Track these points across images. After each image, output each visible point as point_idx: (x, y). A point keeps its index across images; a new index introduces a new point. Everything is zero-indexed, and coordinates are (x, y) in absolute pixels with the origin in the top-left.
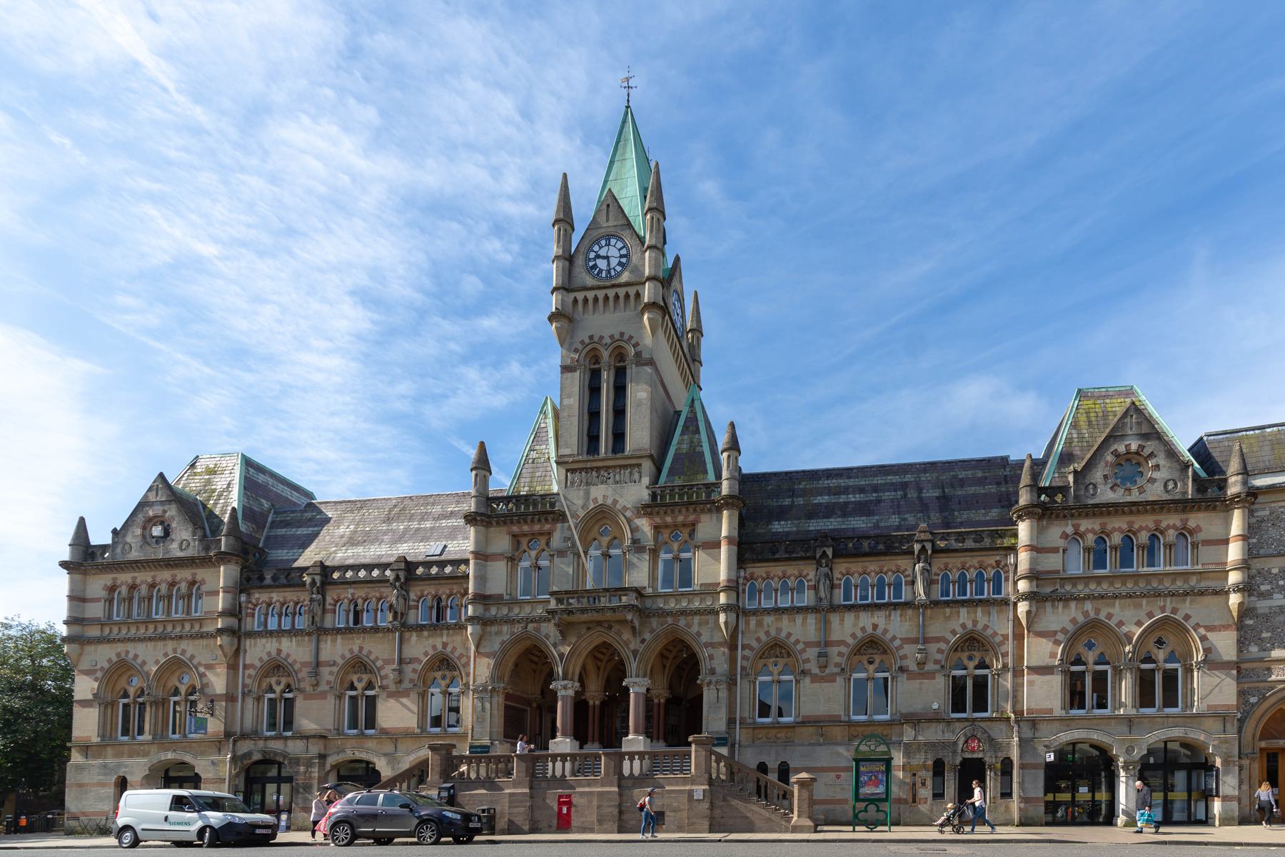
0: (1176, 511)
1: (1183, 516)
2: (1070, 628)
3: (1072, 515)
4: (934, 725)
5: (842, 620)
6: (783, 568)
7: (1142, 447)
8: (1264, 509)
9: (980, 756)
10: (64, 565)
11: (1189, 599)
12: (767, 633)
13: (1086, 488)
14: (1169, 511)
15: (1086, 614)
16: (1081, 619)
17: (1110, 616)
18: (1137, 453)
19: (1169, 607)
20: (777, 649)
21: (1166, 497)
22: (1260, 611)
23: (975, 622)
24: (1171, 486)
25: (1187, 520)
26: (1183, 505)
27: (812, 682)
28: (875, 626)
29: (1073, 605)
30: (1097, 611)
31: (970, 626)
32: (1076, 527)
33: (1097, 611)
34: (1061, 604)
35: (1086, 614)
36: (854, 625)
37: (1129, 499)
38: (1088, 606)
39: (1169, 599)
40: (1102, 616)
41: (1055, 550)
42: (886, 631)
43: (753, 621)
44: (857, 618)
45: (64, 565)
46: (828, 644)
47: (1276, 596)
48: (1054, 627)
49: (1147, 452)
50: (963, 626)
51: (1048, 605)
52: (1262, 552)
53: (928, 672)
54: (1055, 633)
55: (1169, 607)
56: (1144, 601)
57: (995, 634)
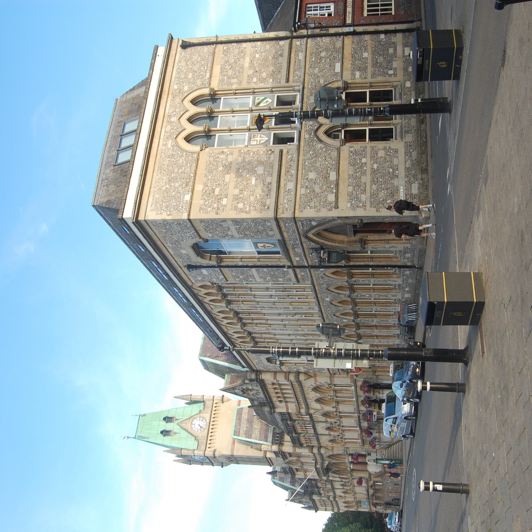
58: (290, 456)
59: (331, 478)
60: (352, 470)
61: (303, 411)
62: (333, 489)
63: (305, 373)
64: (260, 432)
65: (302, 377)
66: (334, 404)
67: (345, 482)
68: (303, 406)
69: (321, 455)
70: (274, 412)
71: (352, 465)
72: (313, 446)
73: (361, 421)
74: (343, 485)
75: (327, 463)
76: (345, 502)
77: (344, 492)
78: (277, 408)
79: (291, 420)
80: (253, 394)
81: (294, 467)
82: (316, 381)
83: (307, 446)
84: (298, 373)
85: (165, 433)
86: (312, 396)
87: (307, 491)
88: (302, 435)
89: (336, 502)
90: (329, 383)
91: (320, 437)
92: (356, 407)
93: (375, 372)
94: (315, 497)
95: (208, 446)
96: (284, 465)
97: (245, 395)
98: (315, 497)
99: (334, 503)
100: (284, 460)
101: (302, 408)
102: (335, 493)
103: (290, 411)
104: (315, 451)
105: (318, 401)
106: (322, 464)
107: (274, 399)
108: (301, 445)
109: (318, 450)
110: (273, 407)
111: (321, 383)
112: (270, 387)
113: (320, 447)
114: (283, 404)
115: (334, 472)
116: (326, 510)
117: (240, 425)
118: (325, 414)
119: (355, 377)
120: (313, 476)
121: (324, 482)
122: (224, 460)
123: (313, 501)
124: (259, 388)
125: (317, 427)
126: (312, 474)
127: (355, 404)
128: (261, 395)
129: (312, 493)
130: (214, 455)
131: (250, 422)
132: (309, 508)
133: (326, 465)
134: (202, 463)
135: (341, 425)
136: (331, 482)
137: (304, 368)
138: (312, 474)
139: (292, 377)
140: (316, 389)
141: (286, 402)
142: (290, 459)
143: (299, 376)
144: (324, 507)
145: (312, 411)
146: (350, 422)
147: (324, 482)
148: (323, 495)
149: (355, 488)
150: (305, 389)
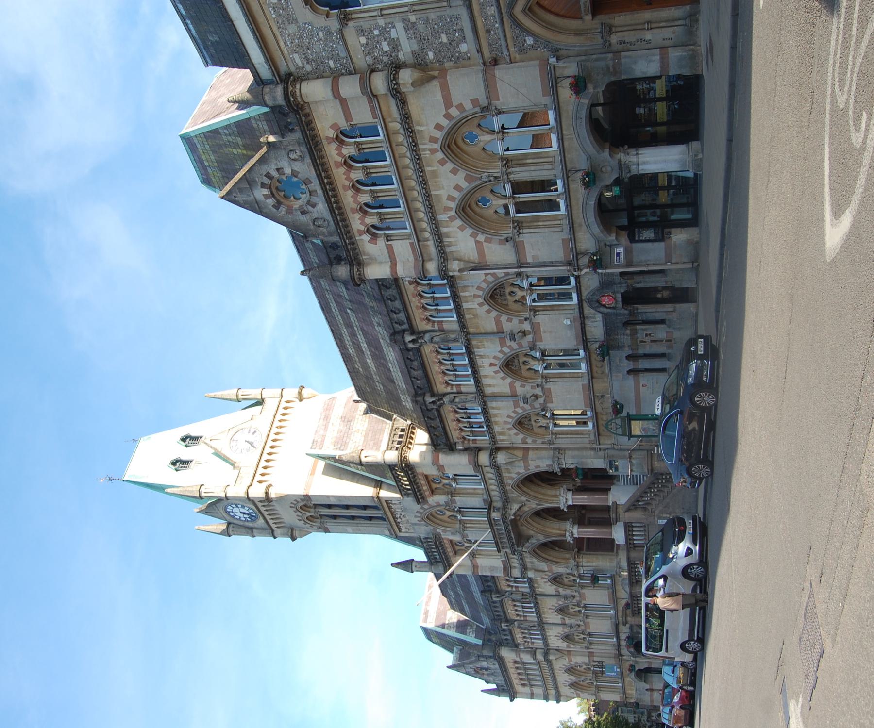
0: (320, 150)
1: (325, 142)
2: (469, 231)
3: (351, 238)
4: (587, 328)
5: (490, 386)
6: (449, 422)
7: (263, 186)
8: (293, 60)
9: (619, 295)
10: (511, 701)
11: (417, 128)
12: (509, 429)
13: (319, 226)
14: (322, 157)
15: (451, 219)
16: (458, 222)
17: (451, 198)
18: (270, 188)
19: (429, 146)
20: (522, 423)
21: (308, 160)
22: (416, 47)
23: (476, 296)
24: (293, 156)
25: (327, 138)
26: (313, 146)
27: (552, 402)
28: (492, 365)
29: (444, 230)
30: (447, 209)
31: (481, 300)
32: (361, 233)
33: (447, 209)
34: (445, 239)
35: (451, 219)
36: (493, 377)
37: (320, 192)
38: (442, 217)
39: (421, 147)
40: (453, 205)
41: (390, 249)
42: (495, 357)
43: (499, 437)
44: (486, 376)
45: (511, 701)
46: (514, 395)
47: (394, 35)
48: (471, 243)
49: (267, 181)
50: (481, 305)
51: (448, 250)
52: (343, 54)
53: (532, 328)
54: (477, 242)
55: (429, 146)
56: (428, 169)
57: (484, 281)
58: (433, 492)
59: (531, 574)
60: (579, 541)
61: (432, 267)
62: (541, 624)
63: (420, 64)
64: (366, 436)
65: (406, 76)
66: (509, 231)
67: (566, 597)
68: (432, 248)
69: (497, 468)
70: (363, 281)
71: (576, 527)
72: (479, 449)
73: (587, 310)
74: (562, 610)
75: (515, 507)
76: (570, 670)
77: (567, 638)
78: (369, 264)
79: (413, 331)
80: (301, 207)
81: (448, 536)
82: (448, 102)
83: (466, 450)
84: (396, 67)
85: (179, 464)
86: (449, 183)
87: (489, 640)
88: (446, 399)
89: (550, 663)
90: (484, 102)
91: (492, 404)
92: (566, 235)
93: (609, 29)
94: (507, 654)
95: (258, 477)
96: (423, 531)
97: (283, 210)
98: (507, 654)
99: (545, 665)
100: (419, 502)
101: (431, 260)
102: (545, 639)
103: (401, 272)
104: (484, 458)
105: (467, 210)
106: (504, 510)
107: (356, 223)
108: (451, 448)
109: (491, 455)
110: (355, 260)
111: (460, 107)
112: (332, 153)
113: (495, 449)
114: (381, 243)
115: (535, 553)
116: (532, 696)
117: (326, 427)
118: (561, 610)
119: (553, 60)
120: (492, 568)
121: (519, 597)
122: (290, 517)
123: (501, 661)
124: (306, 169)
125: (479, 361)
126: (491, 563)
127: (565, 222)
128: (321, 208)
129: (500, 644)
130: (267, 493)
131: (347, 420)
132: (498, 691)
133: (513, 511)
134: (252, 529)
135: (584, 602)
136: (534, 596)
137: (410, 27)
138: (491, 563)
139: (379, 82)
140: (452, 146)
141: (388, 238)
142: (433, 500)
143: (397, 73)
144: (527, 690)
145: (454, 267)
146: (557, 329)
147: (519, 597)
148: (522, 647)
149: (590, 620)
150: (425, 146)
